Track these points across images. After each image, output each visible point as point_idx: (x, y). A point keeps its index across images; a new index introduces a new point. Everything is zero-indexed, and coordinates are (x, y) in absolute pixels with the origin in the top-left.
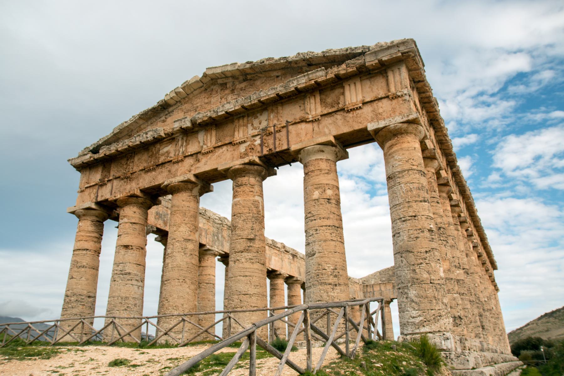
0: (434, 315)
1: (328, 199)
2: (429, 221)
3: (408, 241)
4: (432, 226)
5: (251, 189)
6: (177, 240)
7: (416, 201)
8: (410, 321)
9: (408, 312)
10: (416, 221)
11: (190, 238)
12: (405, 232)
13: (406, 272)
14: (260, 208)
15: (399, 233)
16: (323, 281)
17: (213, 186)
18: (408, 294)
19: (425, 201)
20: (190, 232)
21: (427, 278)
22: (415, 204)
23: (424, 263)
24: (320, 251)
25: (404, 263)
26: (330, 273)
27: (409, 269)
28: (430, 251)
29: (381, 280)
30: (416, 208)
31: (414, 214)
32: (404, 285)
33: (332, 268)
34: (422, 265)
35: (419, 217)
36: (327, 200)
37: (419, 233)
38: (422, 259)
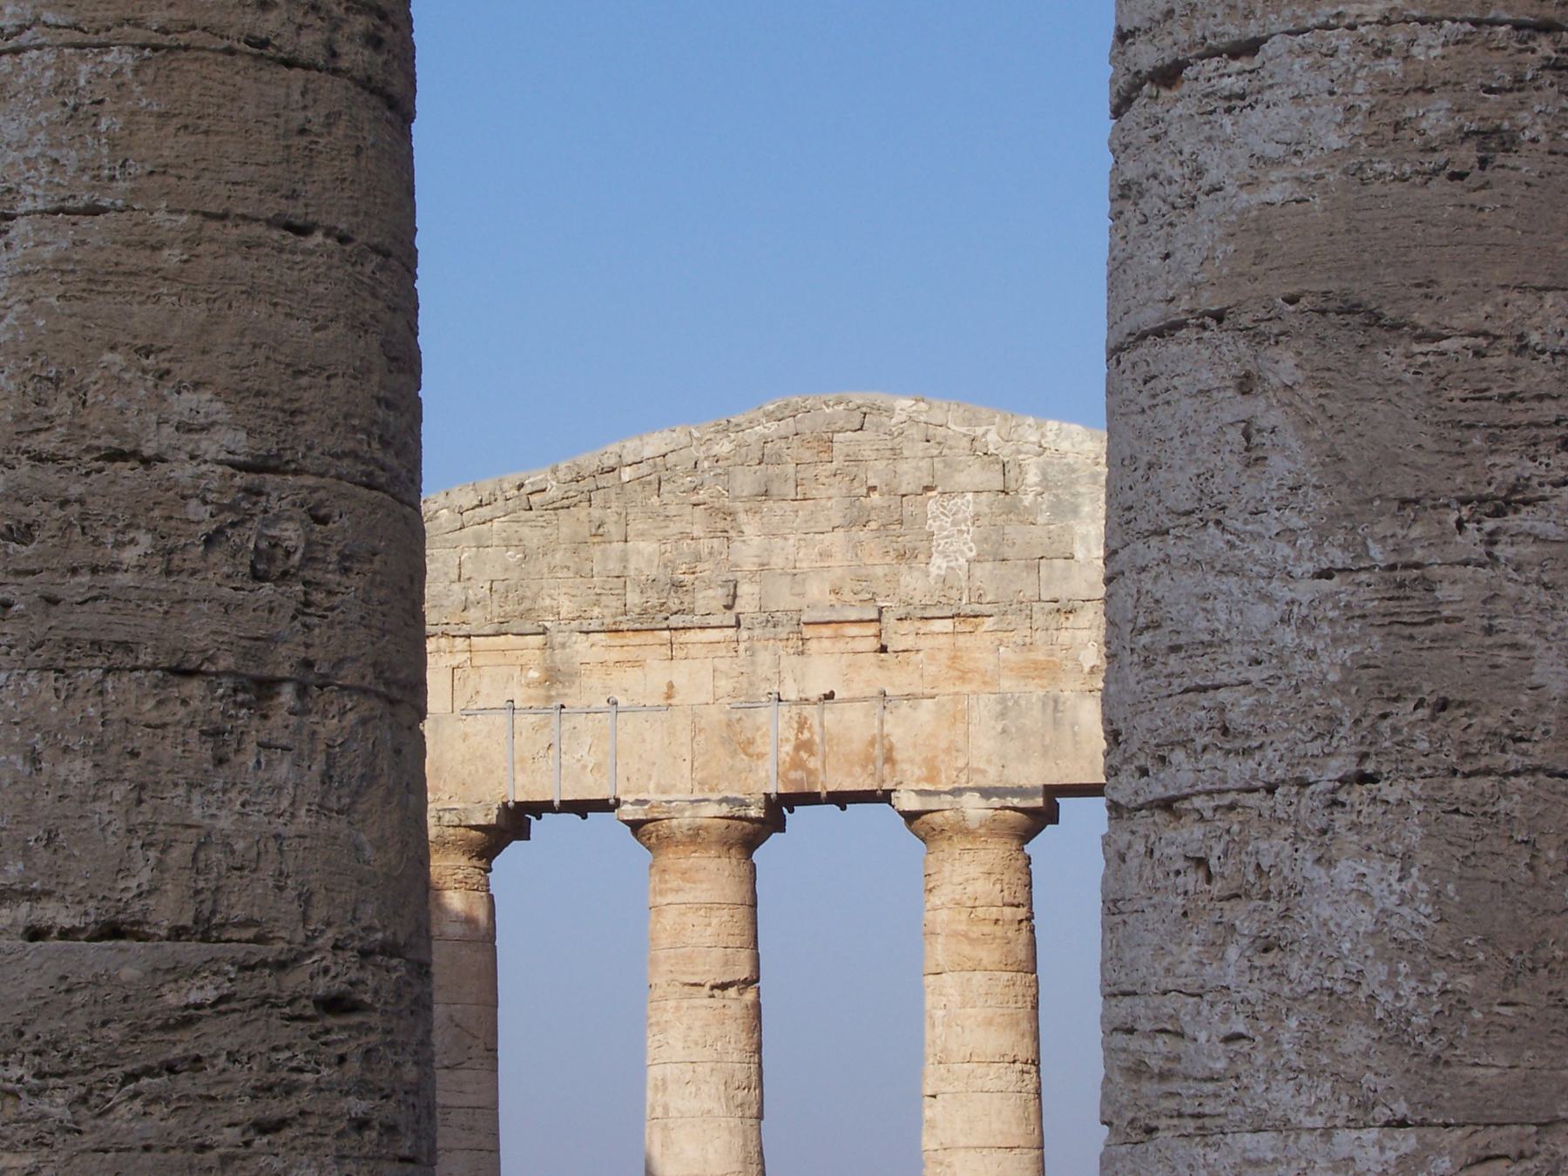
9: (1264, 1145)
12: (1341, 40)
13: (1306, 590)
15: (1250, 47)
25: (1277, 463)
27: (1339, 558)
32: (1237, 770)
33: (239, 443)
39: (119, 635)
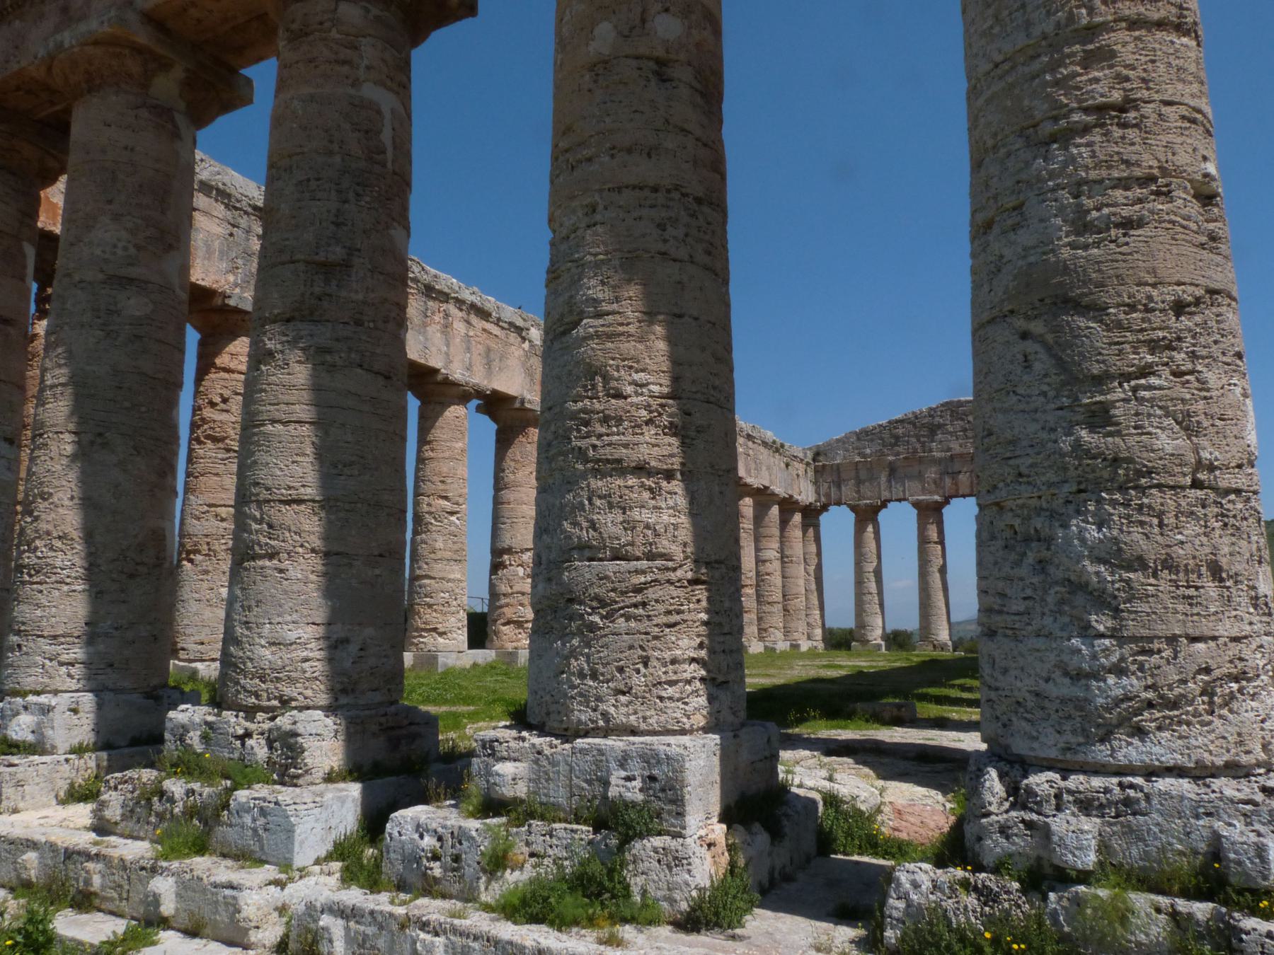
0: (1207, 670)
1: (660, 62)
2: (1196, 138)
3: (1073, 246)
4: (1211, 168)
5: (346, 53)
6: (77, 278)
7: (1134, 24)
8: (1051, 690)
9: (1040, 643)
10: (1132, 134)
11: (134, 272)
14: (386, 136)
16: (607, 453)
17: (249, 82)
18: (1048, 541)
19: (1180, 28)
20: (132, 251)
21: (1178, 457)
22: (1123, 35)
23: (1166, 372)
24: (606, 307)
25: (1037, 366)
26: (644, 413)
28: (1198, 301)
29: (859, 454)
30: (1130, 59)
31: (1117, 96)
34: (1153, 381)
35: (1148, 109)
36: (652, 64)
37: (1140, 201)
38: (1153, 346)
39: (616, 456)
